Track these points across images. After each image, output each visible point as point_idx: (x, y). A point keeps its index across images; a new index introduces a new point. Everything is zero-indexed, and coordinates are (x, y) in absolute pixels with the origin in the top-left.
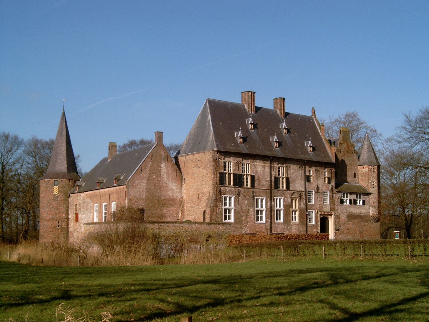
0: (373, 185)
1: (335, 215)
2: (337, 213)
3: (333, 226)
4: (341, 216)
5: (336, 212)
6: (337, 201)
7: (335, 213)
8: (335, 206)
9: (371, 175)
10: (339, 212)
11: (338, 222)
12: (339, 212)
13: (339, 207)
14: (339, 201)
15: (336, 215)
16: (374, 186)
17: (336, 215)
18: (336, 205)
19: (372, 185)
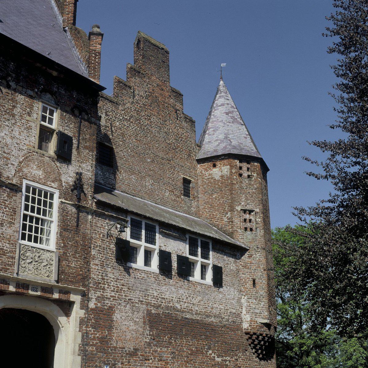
0: (250, 221)
1: (84, 306)
2: (98, 299)
3: (70, 358)
4: (117, 316)
5: (93, 295)
6: (99, 243)
7: (89, 300)
8: (88, 263)
9: (242, 188)
10: (109, 293)
11: (104, 340)
12: (109, 293)
13: (110, 275)
15: (92, 305)
16: (254, 225)
17: (92, 305)
18: (97, 262)
19: (245, 220)
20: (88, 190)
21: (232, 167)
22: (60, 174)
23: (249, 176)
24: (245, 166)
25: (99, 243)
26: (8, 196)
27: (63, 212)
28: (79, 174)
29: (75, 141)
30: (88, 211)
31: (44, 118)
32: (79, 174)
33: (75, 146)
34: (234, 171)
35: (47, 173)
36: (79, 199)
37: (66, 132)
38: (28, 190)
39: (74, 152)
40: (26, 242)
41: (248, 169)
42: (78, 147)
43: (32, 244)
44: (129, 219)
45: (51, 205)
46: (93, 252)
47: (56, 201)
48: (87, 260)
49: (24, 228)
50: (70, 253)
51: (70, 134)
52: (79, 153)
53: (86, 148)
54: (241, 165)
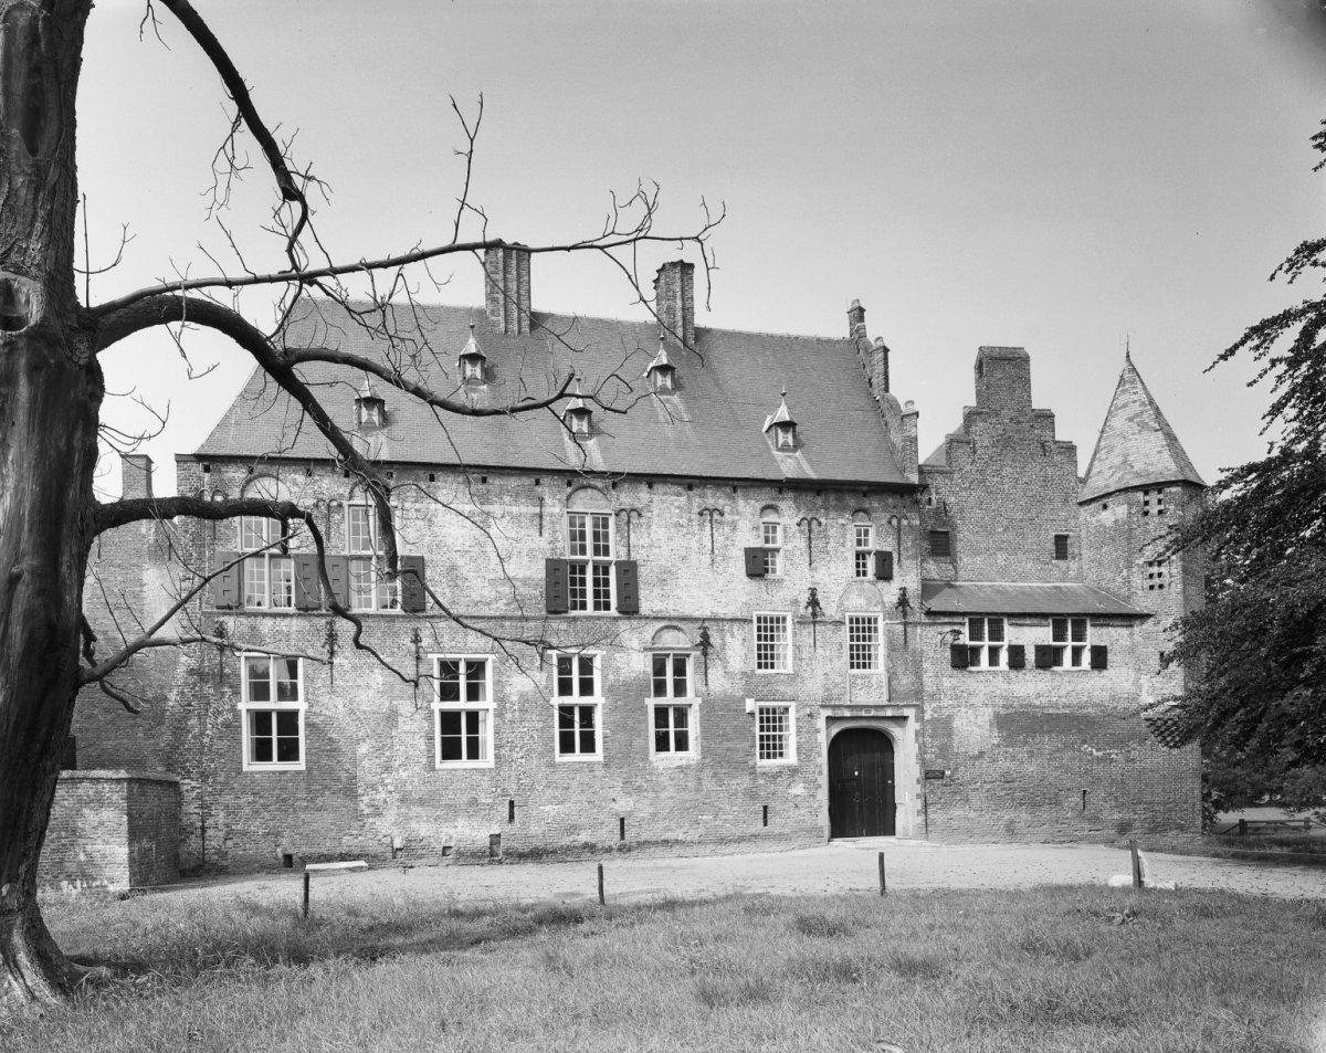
14: (948, 654)
20: (914, 603)
21: (1130, 505)
22: (881, 596)
23: (1160, 512)
24: (1153, 497)
25: (931, 655)
26: (833, 632)
27: (889, 632)
28: (904, 590)
29: (895, 556)
30: (916, 624)
31: (859, 543)
32: (904, 590)
33: (896, 560)
34: (1133, 511)
35: (868, 600)
36: (905, 614)
37: (884, 549)
38: (851, 621)
39: (895, 566)
40: (855, 671)
41: (1160, 502)
42: (899, 560)
43: (862, 671)
44: (966, 620)
45: (876, 629)
46: (925, 665)
47: (881, 625)
48: (918, 674)
49: (852, 657)
50: (900, 670)
51: (889, 549)
52: (900, 566)
53: (908, 558)
54: (1147, 498)
